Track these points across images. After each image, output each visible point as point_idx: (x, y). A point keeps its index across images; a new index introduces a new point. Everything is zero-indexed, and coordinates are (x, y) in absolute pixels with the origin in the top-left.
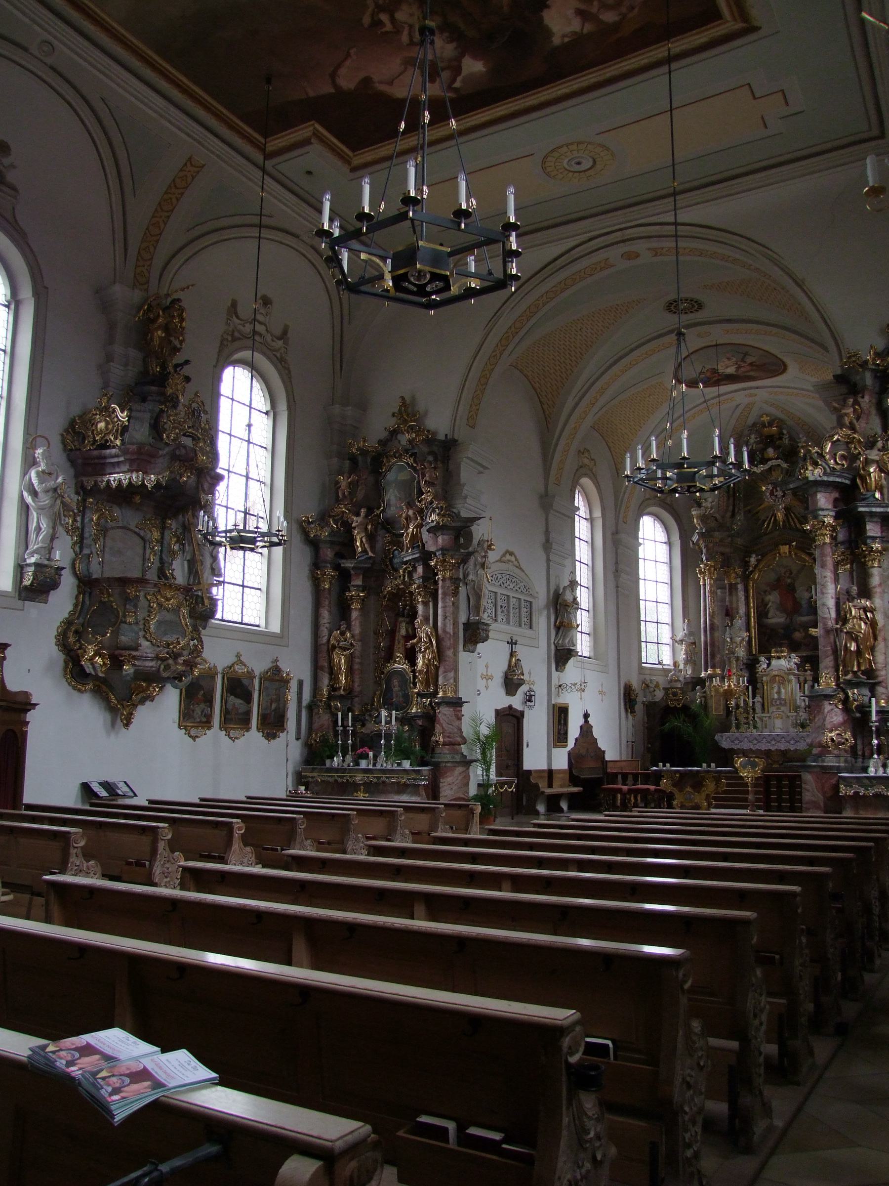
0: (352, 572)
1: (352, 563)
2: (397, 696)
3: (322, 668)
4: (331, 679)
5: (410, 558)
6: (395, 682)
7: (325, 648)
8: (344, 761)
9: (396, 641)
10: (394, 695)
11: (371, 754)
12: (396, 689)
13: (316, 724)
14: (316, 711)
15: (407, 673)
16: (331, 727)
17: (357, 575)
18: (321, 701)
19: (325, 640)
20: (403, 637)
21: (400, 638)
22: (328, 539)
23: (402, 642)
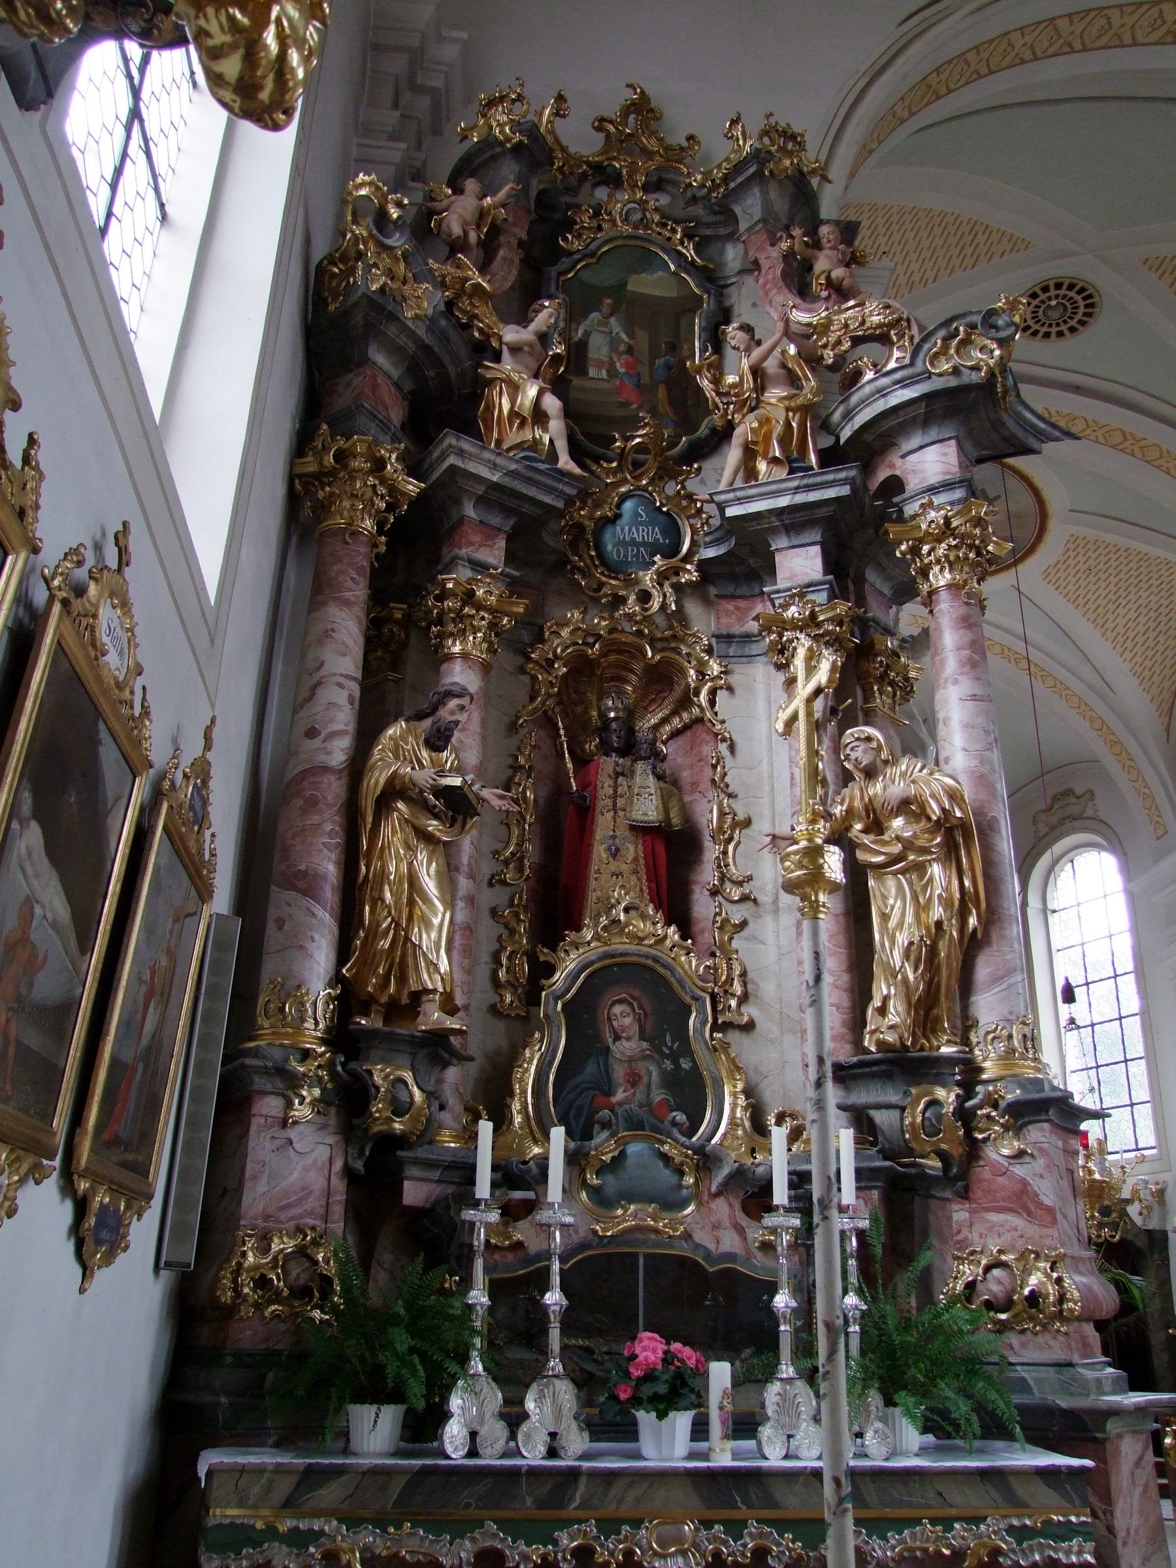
0: (470, 511)
1: (494, 467)
2: (634, 1080)
3: (306, 885)
4: (343, 953)
5: (784, 502)
6: (622, 1016)
7: (334, 790)
8: (514, 1418)
9: (600, 852)
10: (619, 1072)
11: (720, 1373)
12: (628, 1047)
13: (262, 1187)
14: (270, 1106)
15: (680, 982)
16: (338, 1210)
17: (491, 532)
18: (306, 1055)
19: (339, 752)
20: (641, 830)
21: (623, 832)
22: (421, 332)
23: (632, 850)
